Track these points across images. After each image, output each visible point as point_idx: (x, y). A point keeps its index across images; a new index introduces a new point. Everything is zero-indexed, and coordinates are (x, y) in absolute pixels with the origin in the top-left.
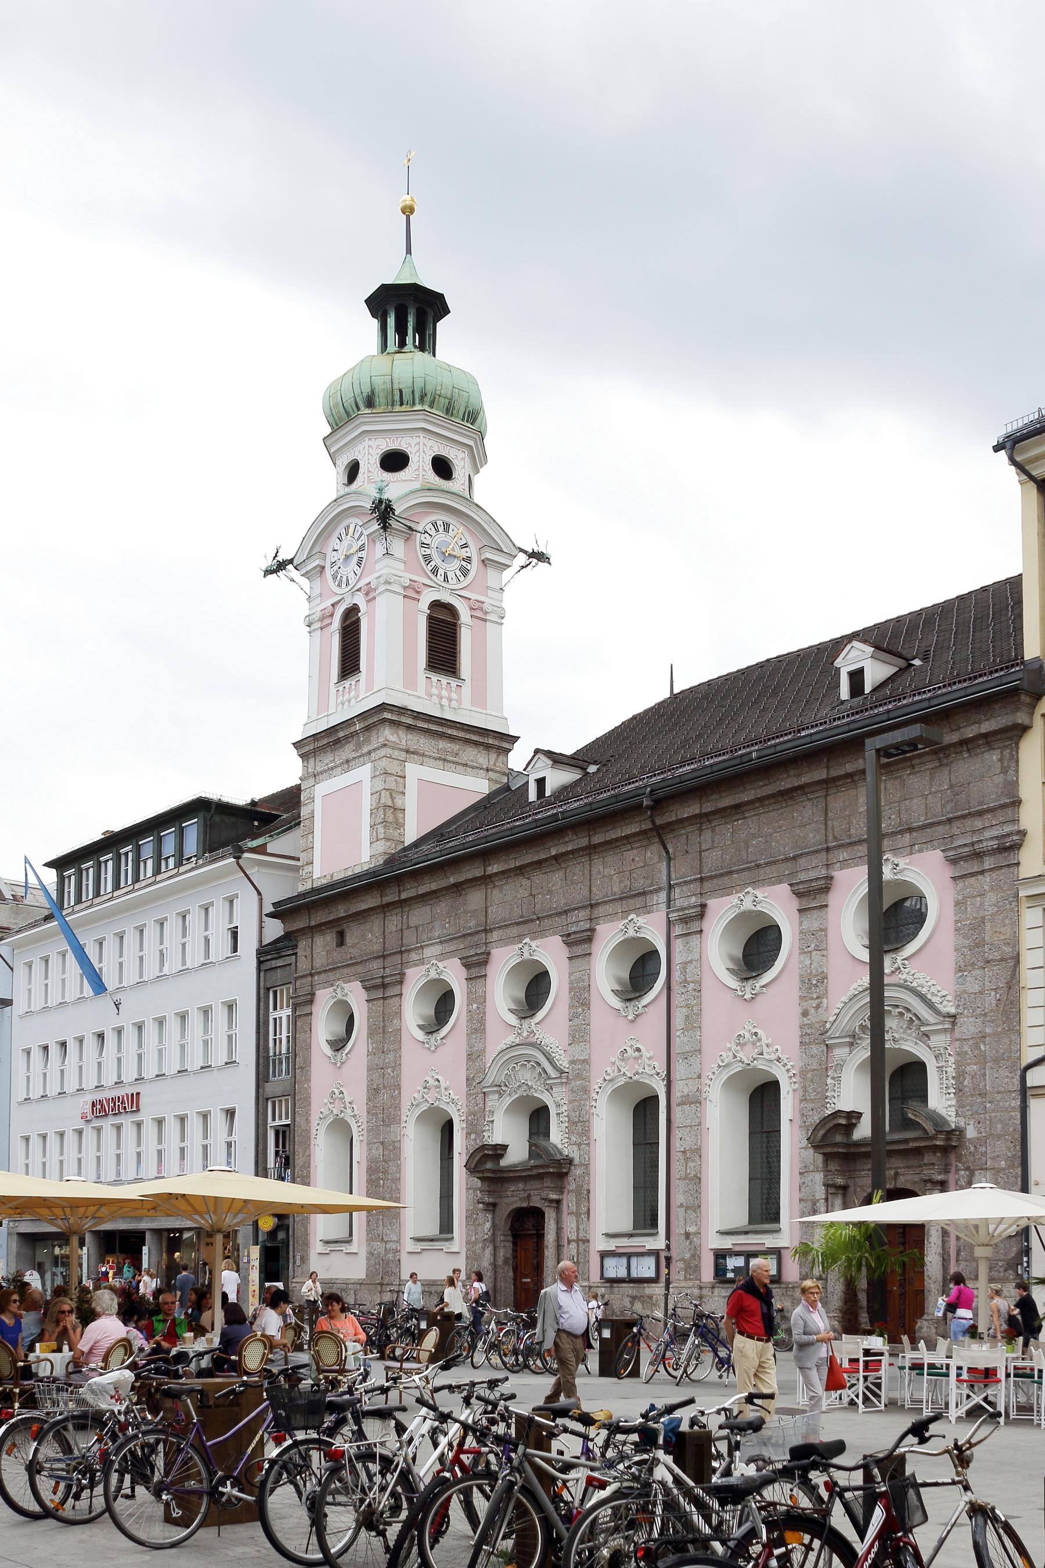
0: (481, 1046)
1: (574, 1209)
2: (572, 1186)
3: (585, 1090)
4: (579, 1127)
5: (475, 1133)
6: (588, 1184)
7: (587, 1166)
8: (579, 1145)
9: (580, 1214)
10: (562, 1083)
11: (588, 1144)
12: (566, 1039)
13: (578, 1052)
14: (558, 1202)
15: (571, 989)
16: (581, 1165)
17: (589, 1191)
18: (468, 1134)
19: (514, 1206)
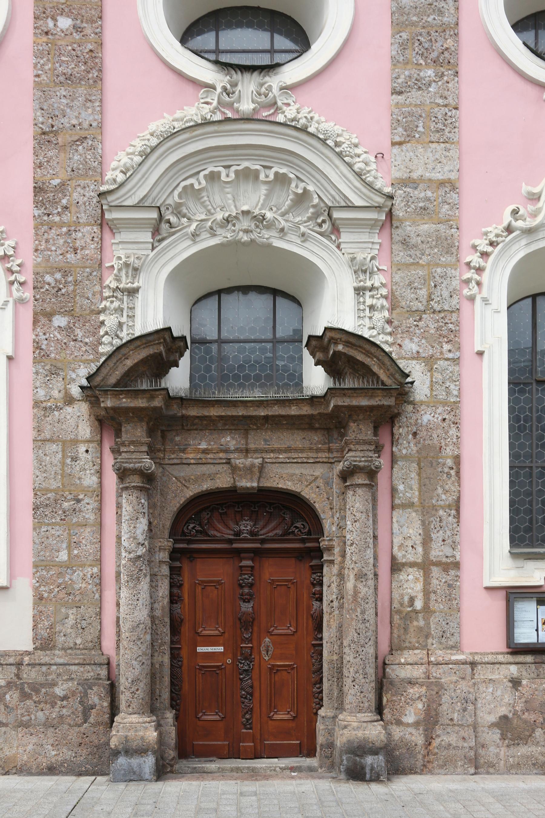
0: (88, 117)
1: (414, 495)
2: (407, 447)
3: (450, 247)
4: (429, 322)
5: (70, 313)
6: (457, 445)
7: (455, 407)
8: (430, 362)
9: (435, 508)
10: (372, 225)
11: (456, 361)
12: (383, 138)
13: (423, 162)
14: (372, 474)
15: (398, 26)
16: (434, 402)
17: (457, 459)
18: (42, 316)
19: (206, 486)
